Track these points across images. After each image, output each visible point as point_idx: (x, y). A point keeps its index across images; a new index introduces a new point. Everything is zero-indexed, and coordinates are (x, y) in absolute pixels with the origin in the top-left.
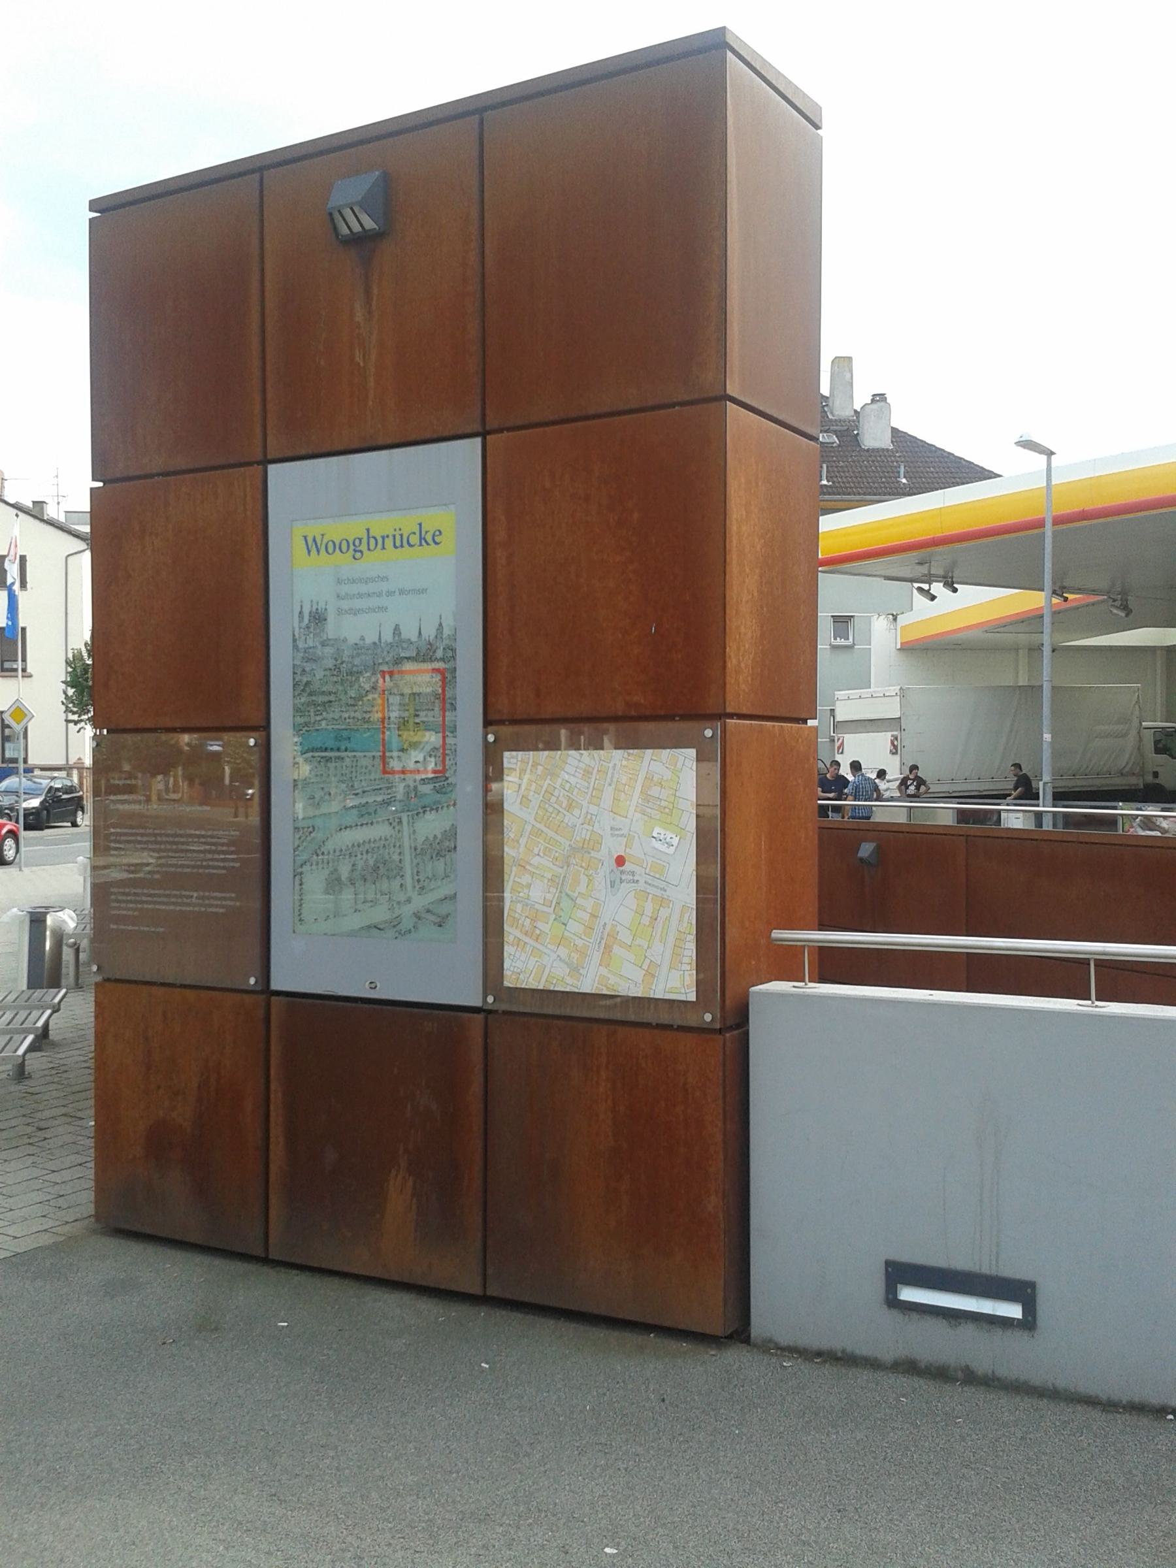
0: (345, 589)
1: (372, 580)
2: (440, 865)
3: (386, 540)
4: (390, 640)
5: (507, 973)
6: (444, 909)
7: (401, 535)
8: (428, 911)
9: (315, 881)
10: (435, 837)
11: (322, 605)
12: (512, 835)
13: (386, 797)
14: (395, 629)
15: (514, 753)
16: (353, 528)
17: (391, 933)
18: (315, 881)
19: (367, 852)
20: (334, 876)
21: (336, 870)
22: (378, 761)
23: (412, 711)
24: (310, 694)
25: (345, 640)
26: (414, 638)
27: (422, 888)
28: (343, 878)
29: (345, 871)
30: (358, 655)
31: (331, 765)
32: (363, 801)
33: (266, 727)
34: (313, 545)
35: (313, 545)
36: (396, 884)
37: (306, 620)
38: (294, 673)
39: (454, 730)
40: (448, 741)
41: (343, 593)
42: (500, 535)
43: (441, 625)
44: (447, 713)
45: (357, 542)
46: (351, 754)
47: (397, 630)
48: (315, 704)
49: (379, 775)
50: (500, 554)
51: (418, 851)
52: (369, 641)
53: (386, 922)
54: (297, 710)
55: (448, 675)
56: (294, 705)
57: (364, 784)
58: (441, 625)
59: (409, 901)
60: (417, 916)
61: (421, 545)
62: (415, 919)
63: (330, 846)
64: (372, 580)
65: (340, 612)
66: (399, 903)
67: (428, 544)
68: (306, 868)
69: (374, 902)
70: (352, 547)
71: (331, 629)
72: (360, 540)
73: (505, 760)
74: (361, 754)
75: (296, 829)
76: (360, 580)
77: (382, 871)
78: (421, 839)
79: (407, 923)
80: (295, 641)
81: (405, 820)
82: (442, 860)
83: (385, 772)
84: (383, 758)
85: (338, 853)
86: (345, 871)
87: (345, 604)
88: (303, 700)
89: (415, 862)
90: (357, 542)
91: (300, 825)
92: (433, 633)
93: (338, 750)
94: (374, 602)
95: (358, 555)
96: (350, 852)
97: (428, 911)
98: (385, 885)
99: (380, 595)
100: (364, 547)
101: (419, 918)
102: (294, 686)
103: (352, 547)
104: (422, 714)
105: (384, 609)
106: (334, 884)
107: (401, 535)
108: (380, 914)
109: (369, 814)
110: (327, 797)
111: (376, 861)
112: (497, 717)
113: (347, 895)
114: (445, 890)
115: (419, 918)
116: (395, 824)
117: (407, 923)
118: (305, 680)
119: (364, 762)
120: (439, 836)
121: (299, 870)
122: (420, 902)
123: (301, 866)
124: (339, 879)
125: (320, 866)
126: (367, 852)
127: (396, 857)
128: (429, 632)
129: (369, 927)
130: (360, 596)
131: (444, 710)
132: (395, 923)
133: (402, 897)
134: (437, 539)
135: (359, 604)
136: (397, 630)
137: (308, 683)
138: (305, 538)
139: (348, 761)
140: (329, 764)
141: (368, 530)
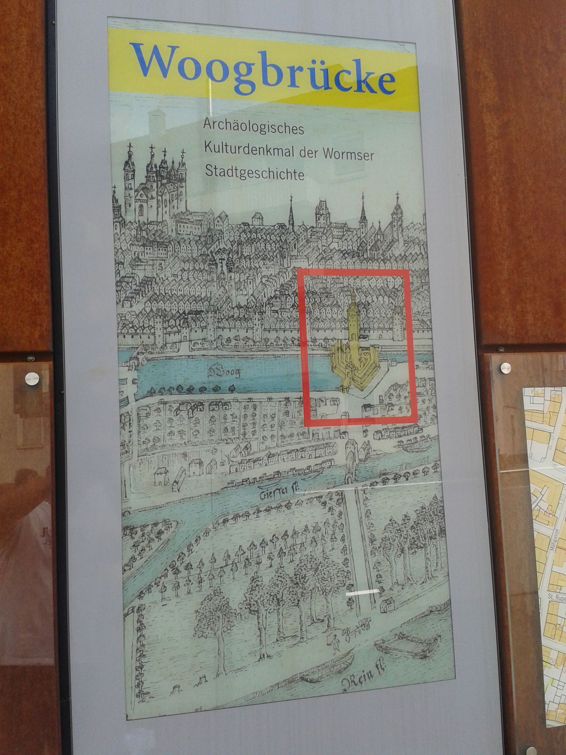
0: (218, 136)
1: (275, 129)
2: (417, 562)
3: (297, 73)
4: (310, 222)
5: (550, 707)
6: (428, 631)
7: (326, 72)
8: (402, 636)
9: (171, 619)
10: (406, 517)
11: (173, 156)
12: (544, 505)
13: (312, 462)
14: (319, 208)
15: (539, 390)
16: (238, 47)
17: (334, 685)
18: (171, 619)
19: (281, 553)
20: (217, 601)
21: (217, 592)
22: (296, 409)
23: (354, 330)
24: (154, 299)
25: (224, 217)
26: (354, 224)
27: (389, 602)
28: (234, 605)
29: (236, 591)
30: (251, 241)
31: (203, 416)
32: (270, 470)
33: (54, 355)
34: (147, 60)
35: (147, 60)
36: (338, 602)
37: (141, 176)
38: (119, 263)
39: (430, 358)
40: (419, 373)
41: (218, 143)
42: (488, 96)
43: (398, 207)
44: (415, 335)
45: (243, 69)
46: (240, 396)
47: (322, 211)
48: (164, 315)
49: (298, 428)
50: (491, 124)
51: (377, 544)
52: (270, 221)
53: (324, 666)
54: (125, 326)
55: (416, 282)
56: (121, 316)
57: (268, 443)
58: (398, 207)
59: (365, 625)
60: (382, 647)
61: (359, 89)
62: (377, 654)
63: (203, 551)
64: (275, 129)
65: (211, 171)
66: (347, 632)
67: (372, 91)
68: (147, 599)
69: (299, 637)
70: (233, 75)
71: (197, 196)
72: (249, 67)
73: (526, 400)
74: (265, 396)
75: (129, 530)
76: (249, 127)
77: (311, 583)
78: (380, 524)
79: (365, 662)
80: (117, 209)
81: (350, 498)
82: (421, 553)
83: (308, 422)
84: (306, 401)
85: (220, 562)
86: (236, 591)
87: (222, 160)
88: (137, 308)
89: (372, 560)
90: (243, 69)
91: (137, 520)
92: (386, 220)
93: (216, 390)
94: (279, 163)
95: (245, 88)
96: (246, 559)
97: (402, 636)
98: (317, 605)
99: (289, 153)
100: (256, 76)
101: (386, 651)
102: (119, 283)
103: (233, 75)
104: (373, 335)
105: (298, 175)
106: (215, 616)
107: (326, 72)
108: (312, 654)
109: (283, 491)
110: (195, 468)
111: (300, 567)
112: (498, 340)
113: (244, 631)
114: (435, 596)
115: (386, 651)
116: (333, 503)
117: (365, 662)
118: (140, 274)
119: (269, 408)
120: (413, 517)
121: (137, 603)
122: (383, 626)
123: (141, 595)
124: (224, 609)
125: (183, 590)
126: (281, 553)
127: (337, 557)
128: (379, 216)
129: (291, 681)
130: (252, 151)
131: (409, 330)
132: (341, 666)
133: (352, 622)
134: (387, 86)
135: (261, 163)
136: (322, 211)
137: (147, 281)
138: (137, 47)
139: (235, 409)
140: (198, 414)
141: (264, 54)
